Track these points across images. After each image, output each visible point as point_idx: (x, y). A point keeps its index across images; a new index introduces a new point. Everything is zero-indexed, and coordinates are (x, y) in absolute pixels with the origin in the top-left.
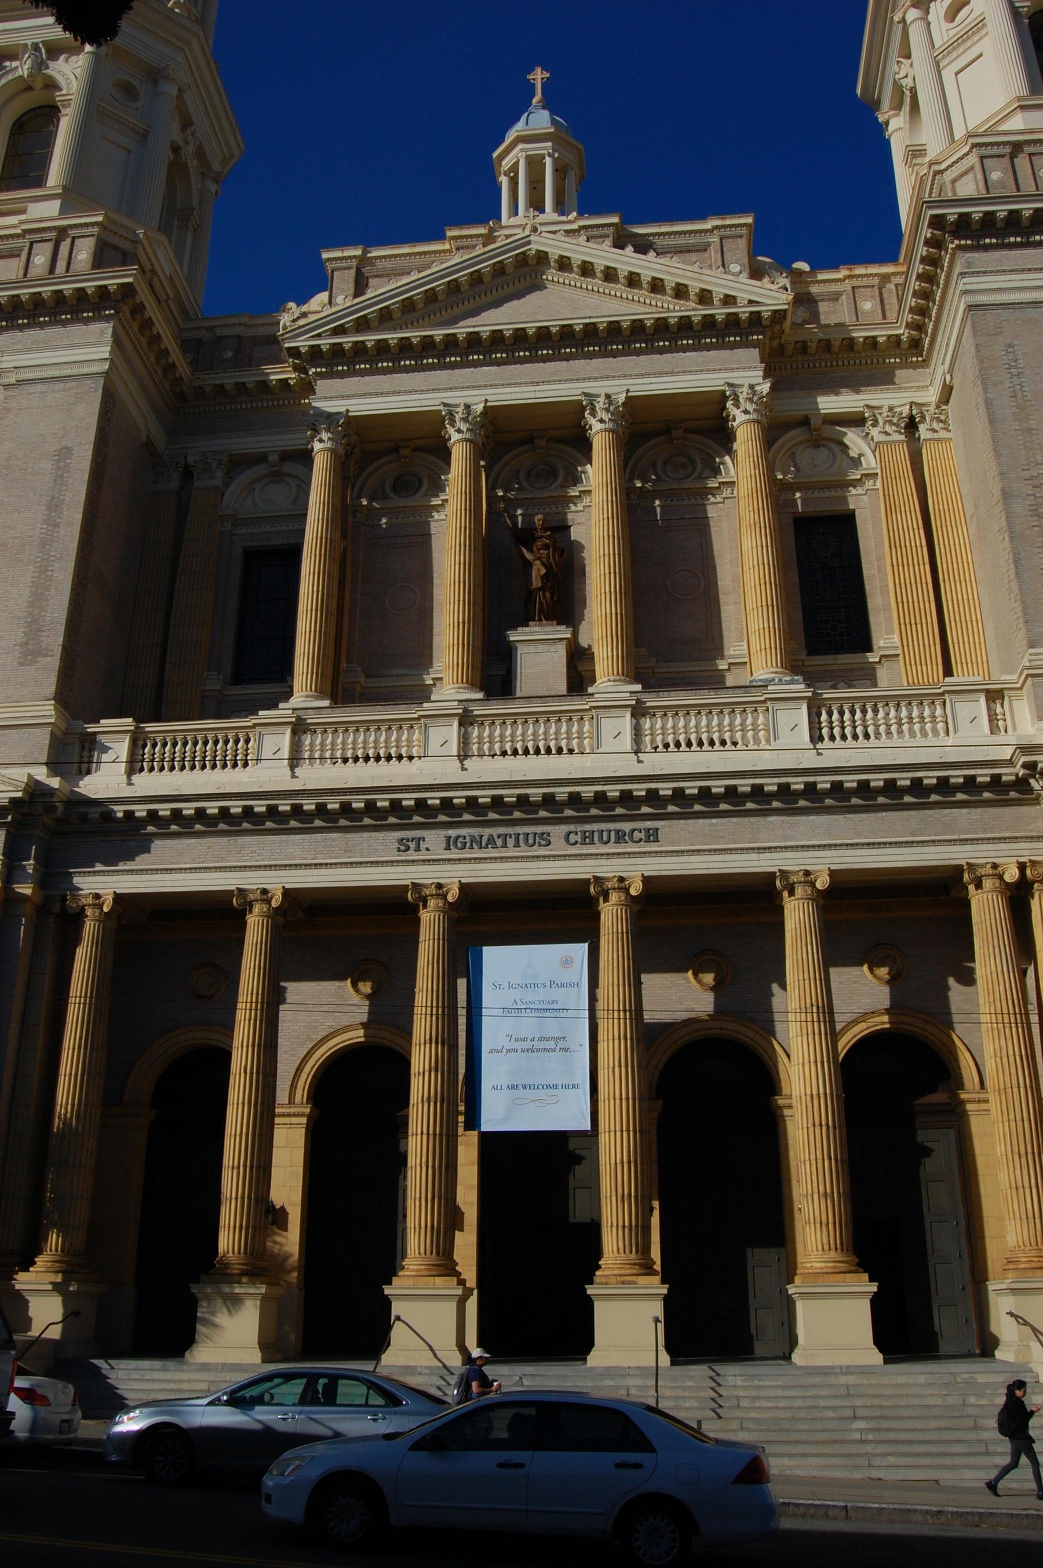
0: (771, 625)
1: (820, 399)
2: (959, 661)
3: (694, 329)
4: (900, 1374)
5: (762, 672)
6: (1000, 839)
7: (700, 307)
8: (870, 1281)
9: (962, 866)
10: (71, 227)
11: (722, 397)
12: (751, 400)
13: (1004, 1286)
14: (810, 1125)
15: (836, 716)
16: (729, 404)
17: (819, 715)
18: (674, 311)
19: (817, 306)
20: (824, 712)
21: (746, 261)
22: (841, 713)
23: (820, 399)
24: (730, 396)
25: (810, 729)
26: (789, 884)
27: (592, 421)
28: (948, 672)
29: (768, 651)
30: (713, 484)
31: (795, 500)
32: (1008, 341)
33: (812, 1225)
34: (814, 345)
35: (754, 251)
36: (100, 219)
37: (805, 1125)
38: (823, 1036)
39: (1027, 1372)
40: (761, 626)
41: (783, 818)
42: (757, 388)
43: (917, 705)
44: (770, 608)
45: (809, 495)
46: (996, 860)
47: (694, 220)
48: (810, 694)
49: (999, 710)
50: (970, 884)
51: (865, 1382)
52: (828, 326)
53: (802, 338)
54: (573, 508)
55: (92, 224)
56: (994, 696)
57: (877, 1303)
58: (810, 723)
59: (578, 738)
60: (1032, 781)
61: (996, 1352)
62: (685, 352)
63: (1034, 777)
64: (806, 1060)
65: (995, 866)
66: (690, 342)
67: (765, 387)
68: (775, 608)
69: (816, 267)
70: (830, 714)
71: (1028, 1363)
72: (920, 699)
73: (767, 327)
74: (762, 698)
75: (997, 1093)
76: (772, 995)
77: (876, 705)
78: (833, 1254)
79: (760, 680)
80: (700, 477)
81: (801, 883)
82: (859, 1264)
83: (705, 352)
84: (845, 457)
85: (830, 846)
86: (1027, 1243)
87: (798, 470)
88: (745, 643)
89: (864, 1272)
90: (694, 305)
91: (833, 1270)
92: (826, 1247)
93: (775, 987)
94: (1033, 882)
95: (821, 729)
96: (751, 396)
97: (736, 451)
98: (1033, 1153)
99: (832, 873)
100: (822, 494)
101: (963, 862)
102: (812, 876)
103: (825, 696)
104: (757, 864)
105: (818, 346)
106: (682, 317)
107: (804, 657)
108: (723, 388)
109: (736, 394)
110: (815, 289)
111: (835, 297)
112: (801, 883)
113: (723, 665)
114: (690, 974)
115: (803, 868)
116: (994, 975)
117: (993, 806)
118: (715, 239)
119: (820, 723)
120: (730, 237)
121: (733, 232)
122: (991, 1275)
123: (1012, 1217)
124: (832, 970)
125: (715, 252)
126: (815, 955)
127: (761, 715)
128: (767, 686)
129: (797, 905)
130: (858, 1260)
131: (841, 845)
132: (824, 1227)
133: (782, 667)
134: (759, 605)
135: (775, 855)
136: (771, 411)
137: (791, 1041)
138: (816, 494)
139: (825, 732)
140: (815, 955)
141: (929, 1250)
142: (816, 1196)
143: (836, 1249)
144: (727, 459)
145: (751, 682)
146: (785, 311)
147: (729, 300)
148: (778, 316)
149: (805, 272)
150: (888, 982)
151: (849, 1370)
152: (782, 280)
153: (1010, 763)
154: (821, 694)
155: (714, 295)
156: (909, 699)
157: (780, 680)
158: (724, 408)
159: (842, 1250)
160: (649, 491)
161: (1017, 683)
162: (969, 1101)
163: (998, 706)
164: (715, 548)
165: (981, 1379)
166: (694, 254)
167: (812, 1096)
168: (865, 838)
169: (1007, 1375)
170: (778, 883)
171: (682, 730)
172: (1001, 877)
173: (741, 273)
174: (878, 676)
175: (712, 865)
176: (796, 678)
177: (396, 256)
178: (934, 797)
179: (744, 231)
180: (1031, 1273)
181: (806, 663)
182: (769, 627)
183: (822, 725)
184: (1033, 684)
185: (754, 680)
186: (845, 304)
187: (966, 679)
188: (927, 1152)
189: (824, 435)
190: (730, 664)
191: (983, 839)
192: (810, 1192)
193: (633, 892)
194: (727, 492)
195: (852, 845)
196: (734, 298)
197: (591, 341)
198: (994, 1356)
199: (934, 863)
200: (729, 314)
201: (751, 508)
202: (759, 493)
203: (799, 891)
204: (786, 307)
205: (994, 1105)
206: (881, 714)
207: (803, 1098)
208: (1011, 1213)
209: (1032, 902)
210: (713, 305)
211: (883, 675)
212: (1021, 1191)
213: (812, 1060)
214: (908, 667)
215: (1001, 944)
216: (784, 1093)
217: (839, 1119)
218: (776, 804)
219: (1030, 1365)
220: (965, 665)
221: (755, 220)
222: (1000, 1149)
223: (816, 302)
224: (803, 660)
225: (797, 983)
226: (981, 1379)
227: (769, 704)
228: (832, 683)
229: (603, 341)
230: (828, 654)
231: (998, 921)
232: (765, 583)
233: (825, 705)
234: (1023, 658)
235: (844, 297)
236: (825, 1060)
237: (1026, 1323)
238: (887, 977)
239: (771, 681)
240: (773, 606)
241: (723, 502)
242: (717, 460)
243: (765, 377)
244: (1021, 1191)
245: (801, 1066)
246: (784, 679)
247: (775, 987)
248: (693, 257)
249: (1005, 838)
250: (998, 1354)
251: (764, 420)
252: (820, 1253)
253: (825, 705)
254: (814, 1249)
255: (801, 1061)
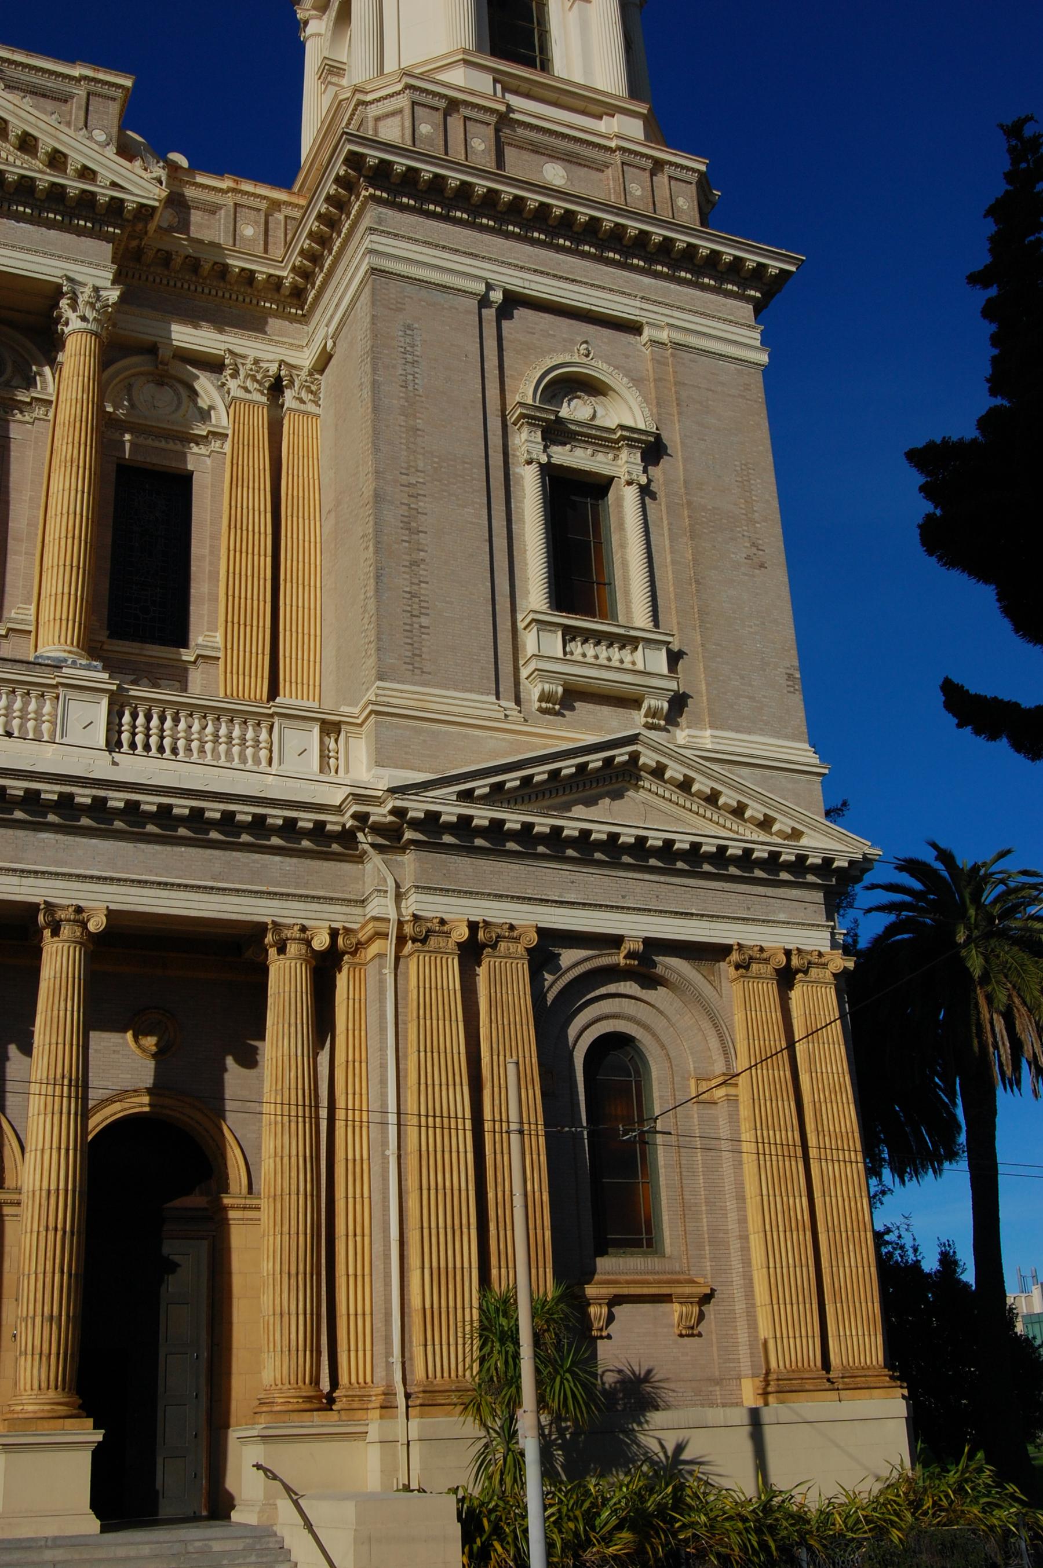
0: (73, 592)
1: (174, 327)
2: (288, 679)
3: (36, 196)
4: (120, 1545)
5: (52, 647)
6: (313, 897)
7: (48, 171)
8: (94, 1429)
9: (266, 924)
10: (671, 163)
11: (55, 293)
12: (92, 306)
13: (255, 1433)
14: (41, 1229)
15: (141, 720)
16: (64, 303)
17: (121, 715)
18: (14, 165)
19: (189, 213)
20: (127, 713)
21: (114, 131)
22: (148, 718)
23: (174, 327)
24: (67, 293)
25: (108, 730)
26: (54, 919)
27: (72, 316)
28: (273, 692)
29: (64, 623)
30: (23, 396)
31: (123, 442)
32: (409, 321)
33: (29, 1357)
34: (179, 260)
35: (126, 121)
36: (703, 168)
37: (35, 1228)
38: (72, 1116)
39: (269, 1536)
40: (60, 591)
41: (59, 837)
42: (102, 293)
43: (240, 724)
44: (75, 569)
45: (141, 440)
46: (306, 923)
47: (59, 59)
48: (114, 687)
49: (333, 746)
50: (271, 947)
51: (76, 1557)
52: (200, 242)
53: (166, 248)
54: (195, 449)
55: (693, 170)
56: (330, 728)
57: (100, 1456)
58: (108, 724)
59: (35, 720)
60: (360, 836)
61: (233, 1513)
62: (18, 222)
63: (363, 831)
64: (47, 1145)
65: (304, 929)
66: (28, 211)
67: (113, 295)
68: (81, 570)
69: (198, 164)
70: (134, 716)
71: (272, 1525)
72: (232, 715)
73: (128, 221)
74: (54, 682)
75: (271, 1200)
76: (7, 1059)
77: (177, 713)
78: (52, 1394)
79: (49, 658)
80: (7, 384)
81: (69, 921)
82: (80, 1407)
83: (44, 229)
84: (191, 405)
85: (112, 879)
86: (286, 1381)
87: (132, 406)
88: (33, 608)
89: (88, 1417)
90: (41, 165)
91: (50, 1415)
92: (44, 1385)
93: (13, 1050)
94: (344, 953)
95: (120, 732)
96: (94, 300)
97: (62, 364)
98: (305, 1274)
99: (110, 914)
100: (157, 444)
101: (268, 920)
102: (85, 915)
103: (132, 693)
104: (17, 890)
105: (212, 268)
106: (23, 177)
107: (104, 639)
108: (60, 281)
109: (74, 293)
110: (190, 192)
111: (212, 210)
112: (69, 921)
113: (187, 655)
114: (129, 1035)
115: (75, 902)
116: (286, 1058)
117: (311, 858)
118: (80, 92)
119: (121, 725)
120: (99, 95)
121: (104, 90)
122: (233, 1420)
123: (272, 1349)
124: (92, 1034)
125: (79, 108)
126: (75, 1013)
127: (48, 702)
128: (61, 667)
129: (60, 948)
130: (81, 1401)
131: (125, 880)
132: (44, 1359)
133: (78, 646)
134: (62, 563)
135: (41, 882)
136: (114, 325)
137: (30, 1120)
138: (149, 442)
139: (125, 737)
140: (75, 1013)
141: (161, 1389)
142: (38, 1320)
143: (56, 1388)
144: (47, 370)
145: (36, 657)
146: (154, 208)
147: (86, 173)
148: (145, 212)
149: (182, 168)
150: (154, 1056)
151: (56, 1542)
152: (158, 169)
153: (338, 810)
154: (128, 690)
155: (70, 161)
156: (218, 713)
157: (74, 662)
158: (56, 306)
159: (64, 1389)
160: (119, 420)
161: (357, 718)
162: (232, 1208)
163: (333, 740)
164: (11, 479)
165: (217, 1547)
166: (49, 101)
167: (49, 1191)
168: (156, 875)
169: (247, 1541)
170: (41, 918)
171: (210, 738)
172: (308, 943)
173: (108, 144)
174: (190, 679)
175: (203, 906)
176: (95, 663)
177: (59, 74)
178: (245, 838)
179: (119, 94)
180: (286, 1417)
181: (105, 647)
182: (70, 594)
183: (123, 728)
184: (376, 722)
185: (41, 657)
186: (222, 221)
187: (293, 702)
188: (172, 1267)
189: (172, 372)
190: (10, 630)
191: (294, 895)
192: (31, 1313)
193: (92, 927)
194: (39, 412)
195: (139, 882)
196: (94, 173)
197: (84, 213)
198: (230, 1518)
199: (234, 917)
200: (84, 191)
201: (70, 440)
202: (84, 424)
203: (66, 931)
204: (156, 204)
205: (266, 1214)
206: (182, 725)
207: (37, 1193)
208: (271, 1345)
209: (338, 976)
210: (65, 172)
211: (196, 678)
212: (286, 1318)
213: (54, 1146)
214: (229, 675)
215: (299, 1022)
216: (6, 1185)
217: (79, 1219)
218: (52, 818)
219: (275, 1528)
220: (294, 685)
221: (135, 84)
222: (267, 1266)
223: (189, 208)
224: (103, 643)
225: (47, 1047)
226: (217, 1547)
227: (61, 690)
228: (133, 677)
229: (38, 203)
230: (133, 640)
231: (299, 994)
232: (73, 538)
233: (130, 705)
234: (367, 690)
235: (223, 212)
236: (71, 1147)
237: (275, 1477)
238: (154, 1049)
239: (62, 661)
240: (79, 568)
241: (33, 424)
242: (34, 368)
243: (114, 282)
244: (286, 1318)
245: (39, 1153)
246: (79, 662)
247: (13, 1050)
248: (49, 105)
249: (319, 898)
250: (235, 1516)
251: (104, 334)
252: (35, 1392)
253: (130, 705)
254: (28, 1387)
255: (40, 1147)
